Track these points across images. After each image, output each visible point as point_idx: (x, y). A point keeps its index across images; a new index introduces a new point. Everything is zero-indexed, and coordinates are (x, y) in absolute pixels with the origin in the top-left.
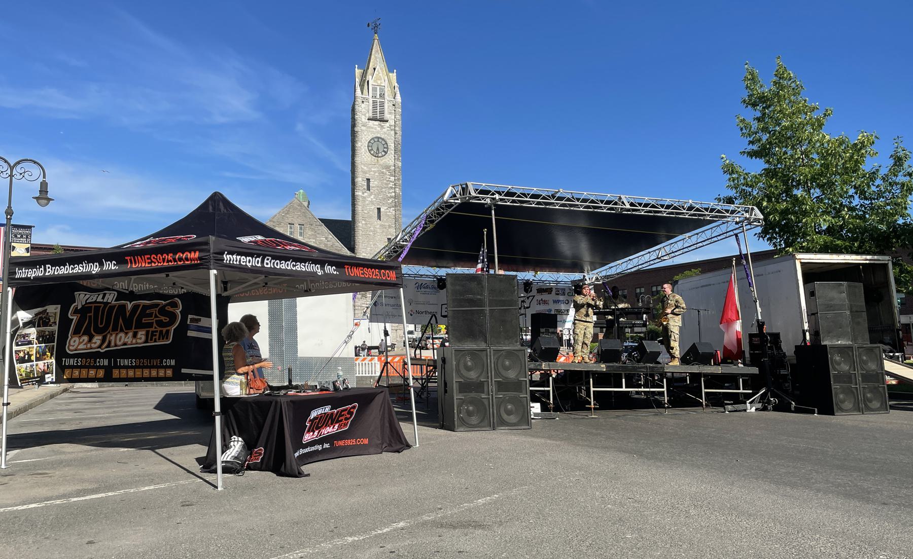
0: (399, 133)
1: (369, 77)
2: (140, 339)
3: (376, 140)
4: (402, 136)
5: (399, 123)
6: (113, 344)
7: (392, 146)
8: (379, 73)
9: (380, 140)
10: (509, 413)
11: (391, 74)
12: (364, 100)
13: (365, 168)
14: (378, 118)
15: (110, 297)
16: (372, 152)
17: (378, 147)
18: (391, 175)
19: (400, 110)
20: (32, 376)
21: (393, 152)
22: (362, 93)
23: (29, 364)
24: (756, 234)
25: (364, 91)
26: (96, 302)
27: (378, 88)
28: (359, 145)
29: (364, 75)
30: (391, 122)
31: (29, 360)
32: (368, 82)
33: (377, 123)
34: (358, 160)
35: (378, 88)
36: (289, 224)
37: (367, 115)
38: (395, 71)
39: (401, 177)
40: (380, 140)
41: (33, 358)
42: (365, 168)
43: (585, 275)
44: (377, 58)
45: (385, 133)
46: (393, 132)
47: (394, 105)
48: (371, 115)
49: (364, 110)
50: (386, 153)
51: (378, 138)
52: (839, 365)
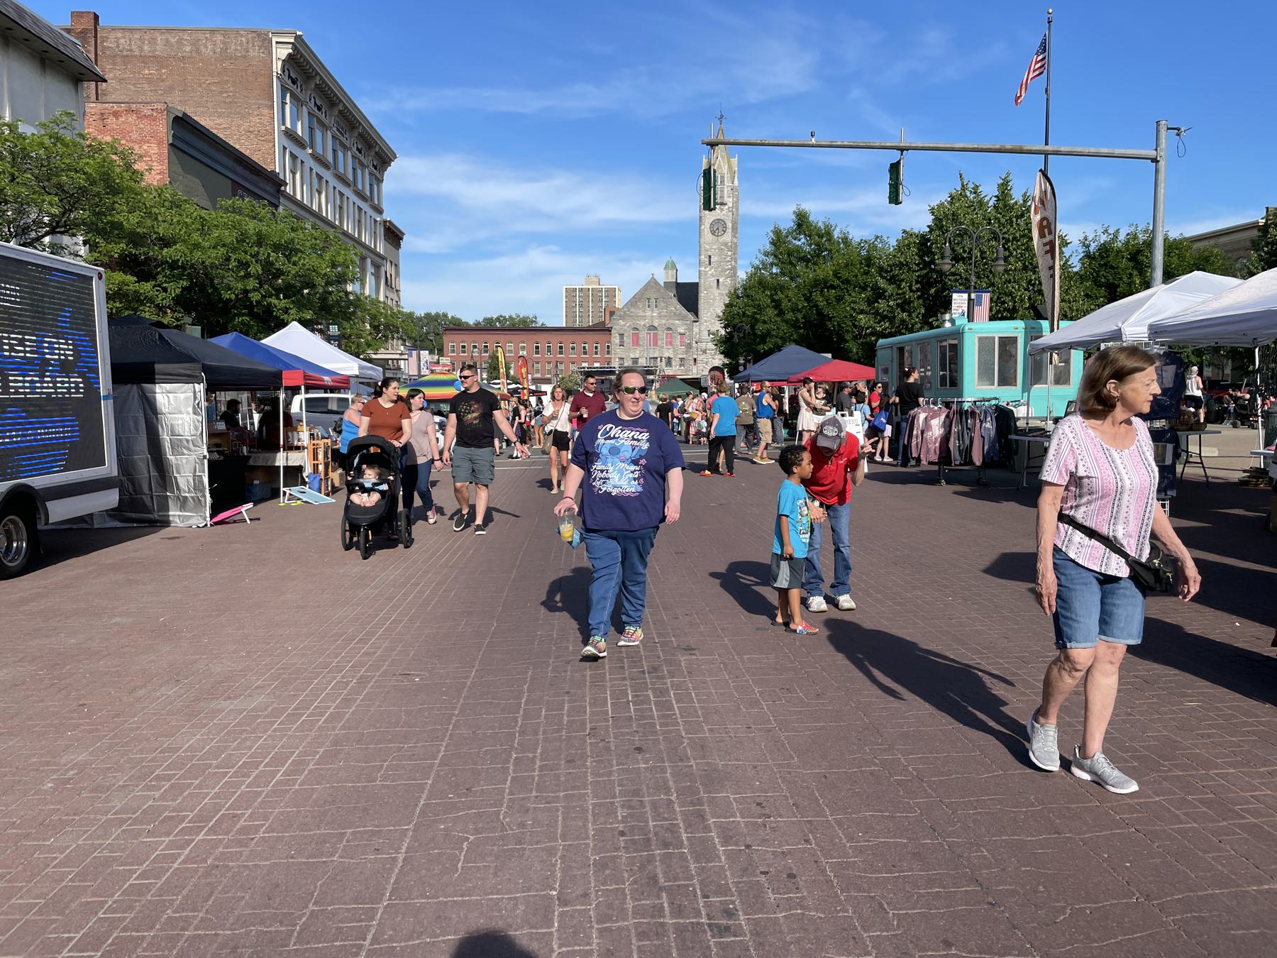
7: (729, 225)
18: (729, 251)
51: (718, 220)
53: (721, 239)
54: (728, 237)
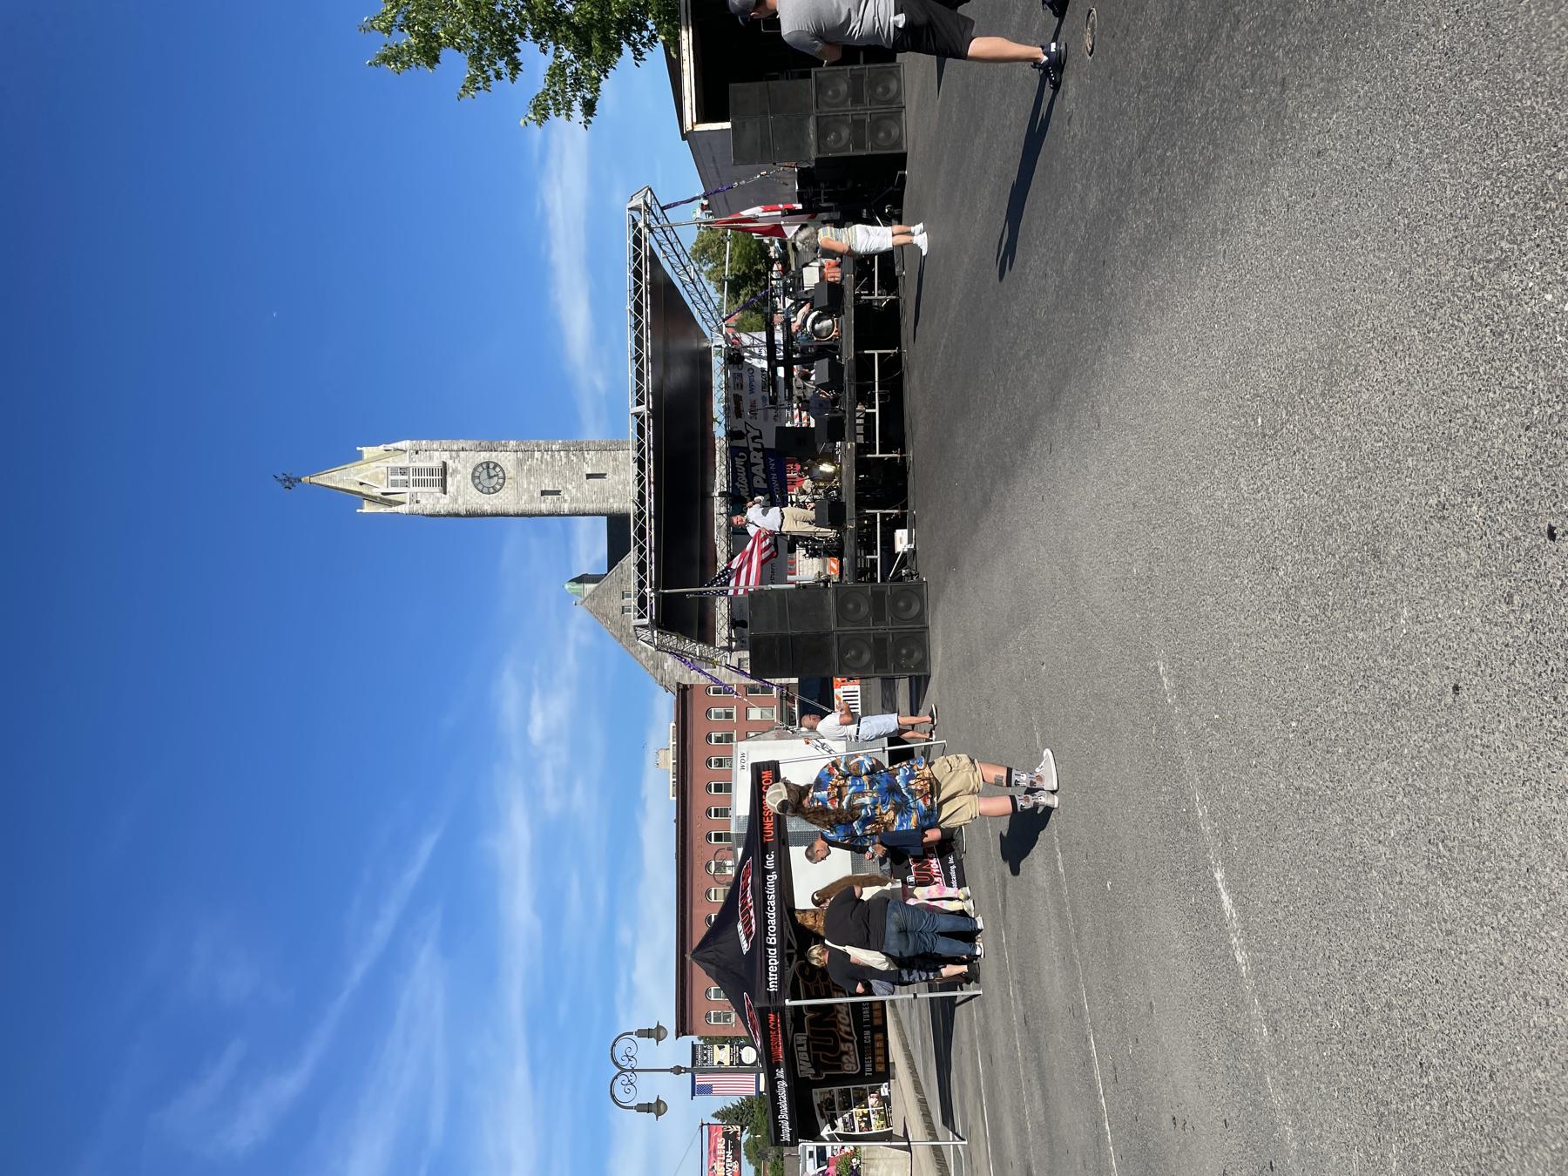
0: (462, 443)
1: (376, 492)
2: (849, 1047)
3: (477, 481)
4: (466, 438)
5: (446, 443)
6: (848, 1029)
7: (484, 456)
8: (367, 476)
9: (477, 474)
10: (908, 607)
11: (365, 456)
12: (415, 500)
13: (525, 498)
14: (440, 477)
15: (801, 1038)
16: (498, 487)
17: (487, 478)
18: (532, 457)
19: (424, 442)
20: (883, 1113)
21: (494, 454)
22: (403, 503)
23: (872, 1116)
24: (637, 65)
25: (399, 499)
26: (808, 1052)
27: (391, 478)
28: (488, 508)
29: (372, 499)
30: (445, 457)
31: (868, 1115)
32: (383, 494)
33: (449, 479)
34: (512, 509)
35: (391, 478)
36: (623, 613)
37: (438, 495)
38: (358, 449)
39: (534, 442)
40: (477, 474)
41: (865, 1111)
42: (525, 498)
43: (713, 345)
44: (342, 478)
45: (465, 467)
46: (462, 454)
47: (417, 453)
48: (437, 489)
49: (431, 501)
50: (496, 465)
51: (473, 477)
52: (842, 143)
53: (510, 470)
54: (507, 459)
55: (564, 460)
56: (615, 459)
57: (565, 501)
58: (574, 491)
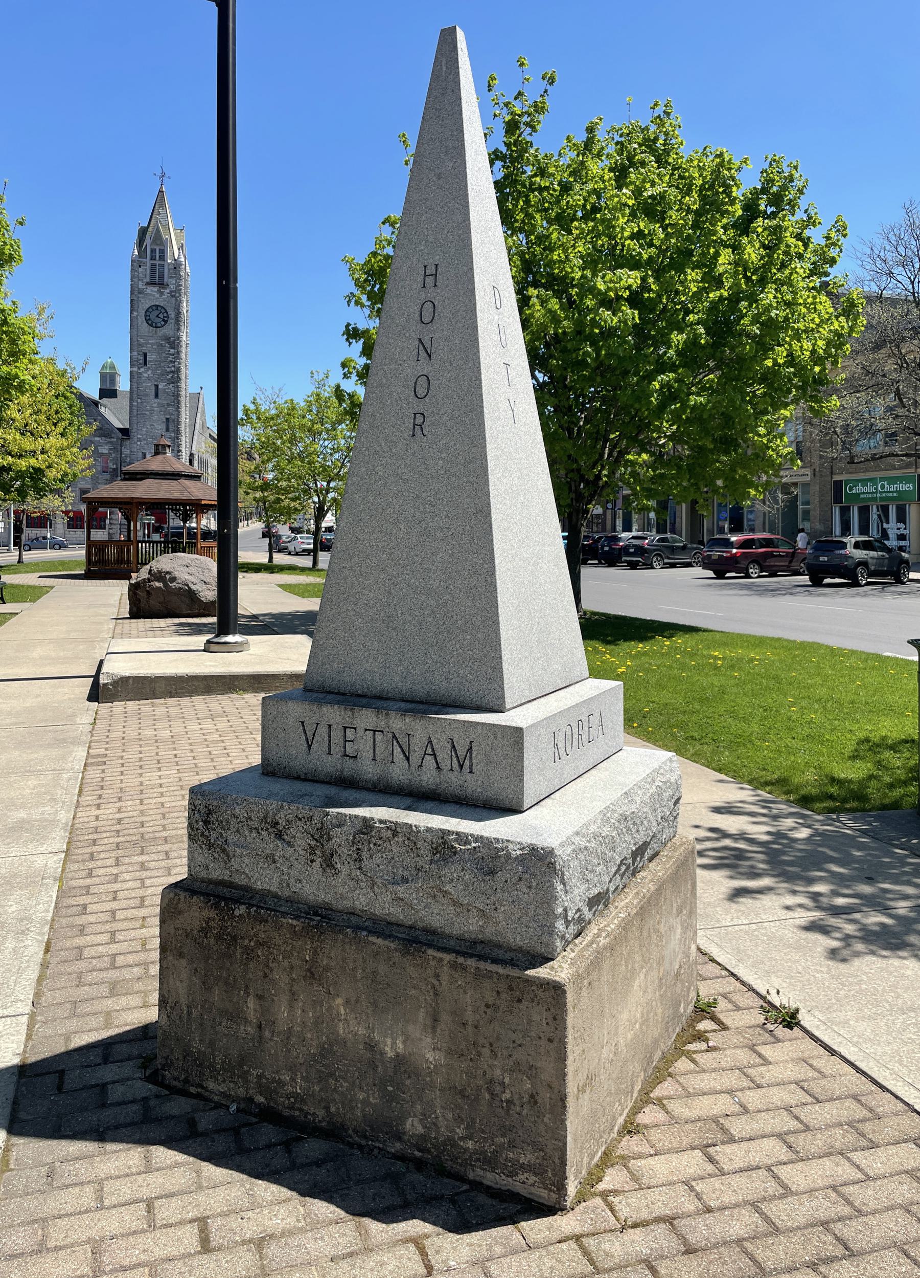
7: (172, 314)
13: (142, 340)
21: (173, 321)
42: (142, 340)
45: (164, 300)
48: (148, 280)
50: (166, 322)
55: (168, 370)
56: (168, 405)
57: (139, 369)
58: (146, 375)
